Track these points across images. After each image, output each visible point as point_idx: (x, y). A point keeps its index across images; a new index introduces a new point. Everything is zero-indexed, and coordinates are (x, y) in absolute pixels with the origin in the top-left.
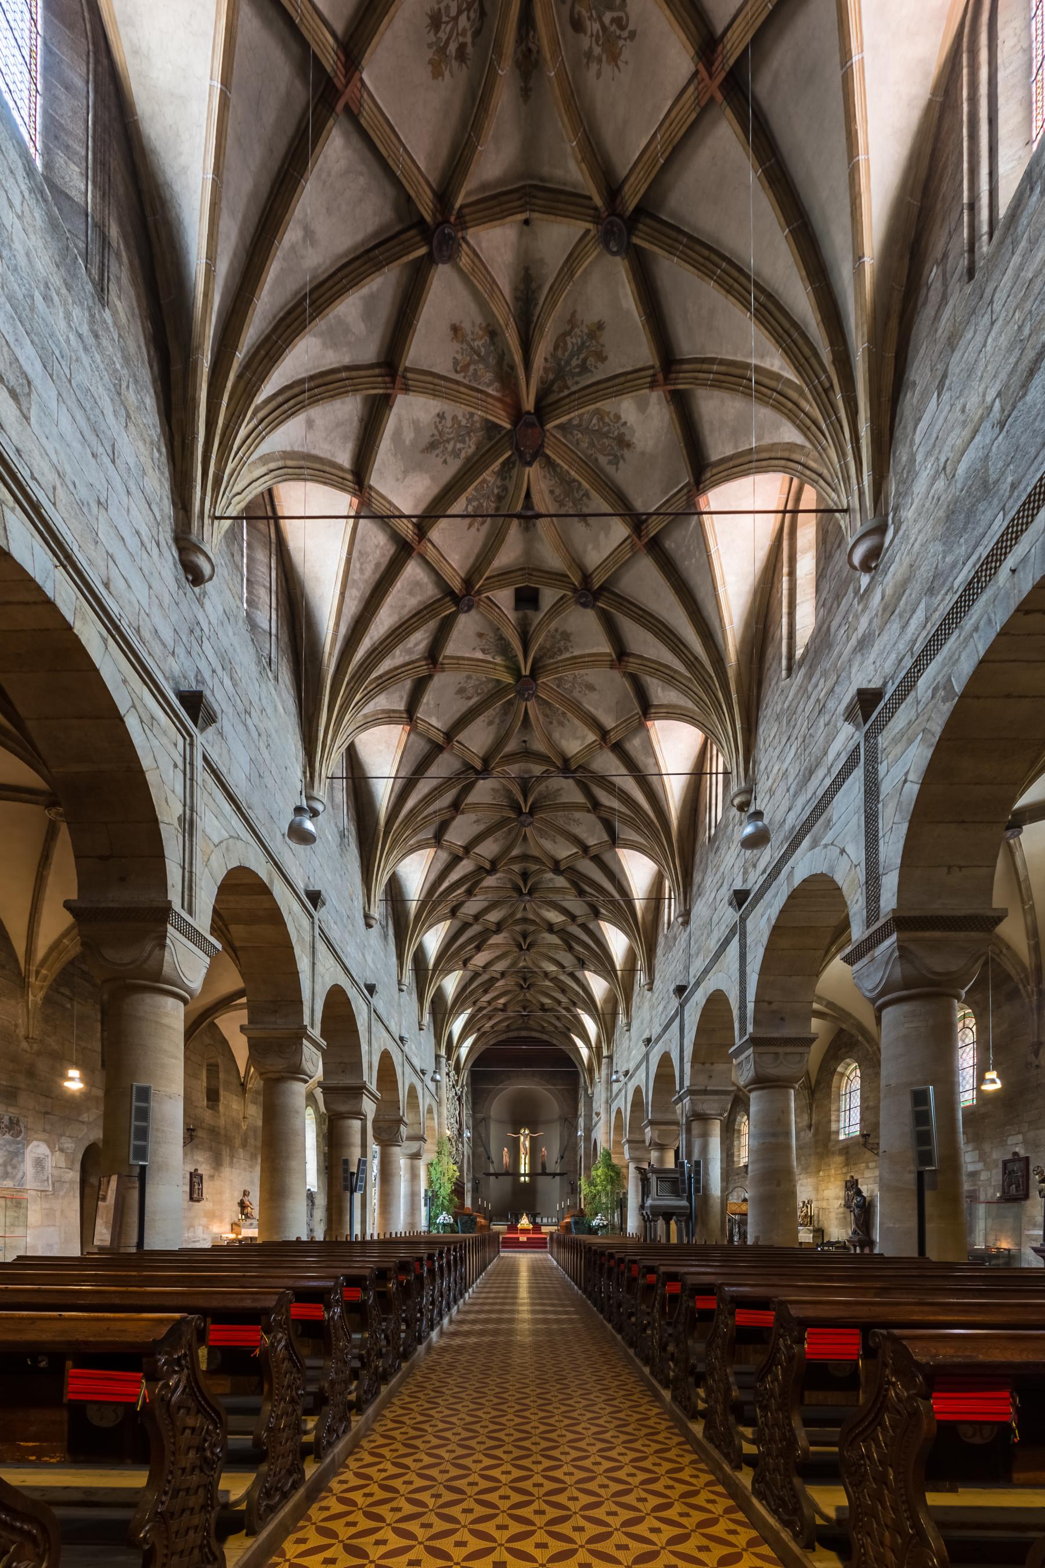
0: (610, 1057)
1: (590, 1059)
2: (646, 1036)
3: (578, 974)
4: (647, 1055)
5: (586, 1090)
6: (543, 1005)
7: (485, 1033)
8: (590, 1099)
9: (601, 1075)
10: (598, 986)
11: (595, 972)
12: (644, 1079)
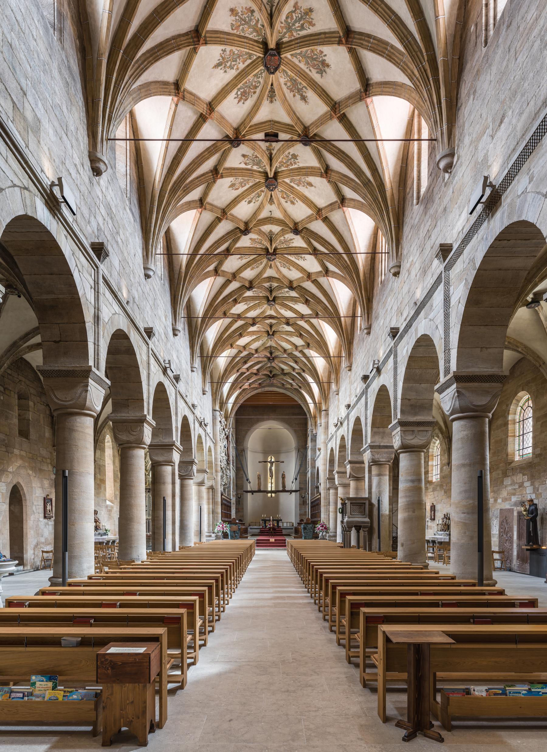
0: (326, 410)
4: (348, 414)
6: (283, 370)
7: (244, 390)
9: (322, 421)
10: (320, 363)
12: (346, 431)
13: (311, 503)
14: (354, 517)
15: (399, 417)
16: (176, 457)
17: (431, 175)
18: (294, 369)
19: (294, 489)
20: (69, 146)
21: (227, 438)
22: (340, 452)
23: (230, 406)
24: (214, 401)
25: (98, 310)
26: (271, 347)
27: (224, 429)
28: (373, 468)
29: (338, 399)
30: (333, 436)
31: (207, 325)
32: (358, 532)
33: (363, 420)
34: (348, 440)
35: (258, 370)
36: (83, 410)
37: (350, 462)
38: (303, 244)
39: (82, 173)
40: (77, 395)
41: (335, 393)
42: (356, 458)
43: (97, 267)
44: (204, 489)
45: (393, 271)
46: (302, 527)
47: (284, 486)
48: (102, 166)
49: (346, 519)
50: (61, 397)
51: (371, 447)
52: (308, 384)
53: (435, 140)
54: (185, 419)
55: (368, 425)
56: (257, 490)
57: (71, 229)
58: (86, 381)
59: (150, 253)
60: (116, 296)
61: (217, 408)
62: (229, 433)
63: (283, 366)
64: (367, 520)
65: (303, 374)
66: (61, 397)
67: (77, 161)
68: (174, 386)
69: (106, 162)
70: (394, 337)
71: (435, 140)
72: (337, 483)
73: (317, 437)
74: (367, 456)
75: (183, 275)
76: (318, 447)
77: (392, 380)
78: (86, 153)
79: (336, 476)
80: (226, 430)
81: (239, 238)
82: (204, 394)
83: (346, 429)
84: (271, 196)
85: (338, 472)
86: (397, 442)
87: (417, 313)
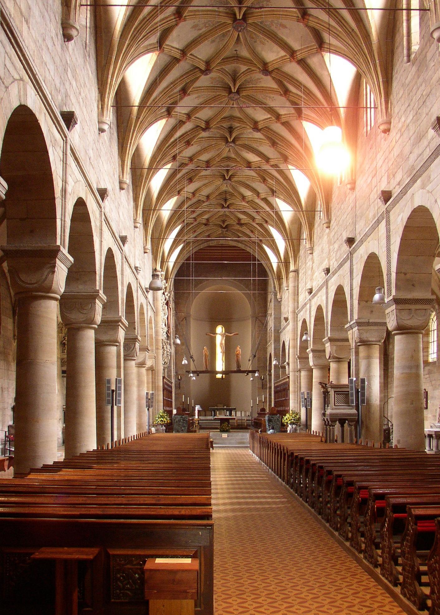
0: (297, 271)
1: (278, 267)
2: (325, 265)
3: (270, 199)
4: (326, 282)
5: (276, 295)
6: (239, 220)
7: (189, 243)
8: (279, 303)
9: (288, 285)
10: (287, 212)
11: (284, 201)
12: (325, 300)
13: (275, 387)
14: (339, 409)
15: (394, 292)
16: (121, 334)
17: (423, 38)
18: (254, 219)
19: (250, 369)
20: (48, 22)
21: (167, 304)
22: (315, 325)
23: (171, 265)
24: (155, 259)
25: (66, 183)
26: (226, 192)
27: (164, 293)
28: (361, 349)
29: (312, 259)
30: (306, 304)
31: (153, 173)
32: (342, 426)
33: (347, 290)
34: (327, 312)
35: (208, 220)
36: (48, 292)
37: (331, 340)
38: (274, 85)
39: (56, 43)
40: (44, 277)
41: (309, 252)
42: (337, 335)
43: (66, 137)
44: (143, 370)
45: (382, 127)
46: (267, 418)
47: (239, 366)
48: (74, 33)
49: (328, 411)
50: (29, 279)
51: (359, 324)
52: (271, 236)
53: (429, 10)
54: (129, 287)
55: (354, 297)
56: (204, 369)
57: (50, 106)
58: (53, 262)
59: (106, 106)
60: (78, 163)
61: (158, 268)
62: (169, 297)
63: (241, 216)
64: (354, 411)
65: (265, 225)
66: (29, 279)
67: (53, 34)
68: (121, 249)
69: (78, 28)
70: (386, 200)
71: (429, 10)
72: (311, 363)
73: (283, 302)
74: (353, 334)
75: (134, 121)
76: (283, 316)
77: (384, 249)
78: (60, 22)
79: (311, 355)
80: (166, 294)
81: (198, 78)
82: (145, 253)
83: (324, 298)
84: (238, 35)
85: (313, 351)
86: (391, 322)
87: (413, 181)
